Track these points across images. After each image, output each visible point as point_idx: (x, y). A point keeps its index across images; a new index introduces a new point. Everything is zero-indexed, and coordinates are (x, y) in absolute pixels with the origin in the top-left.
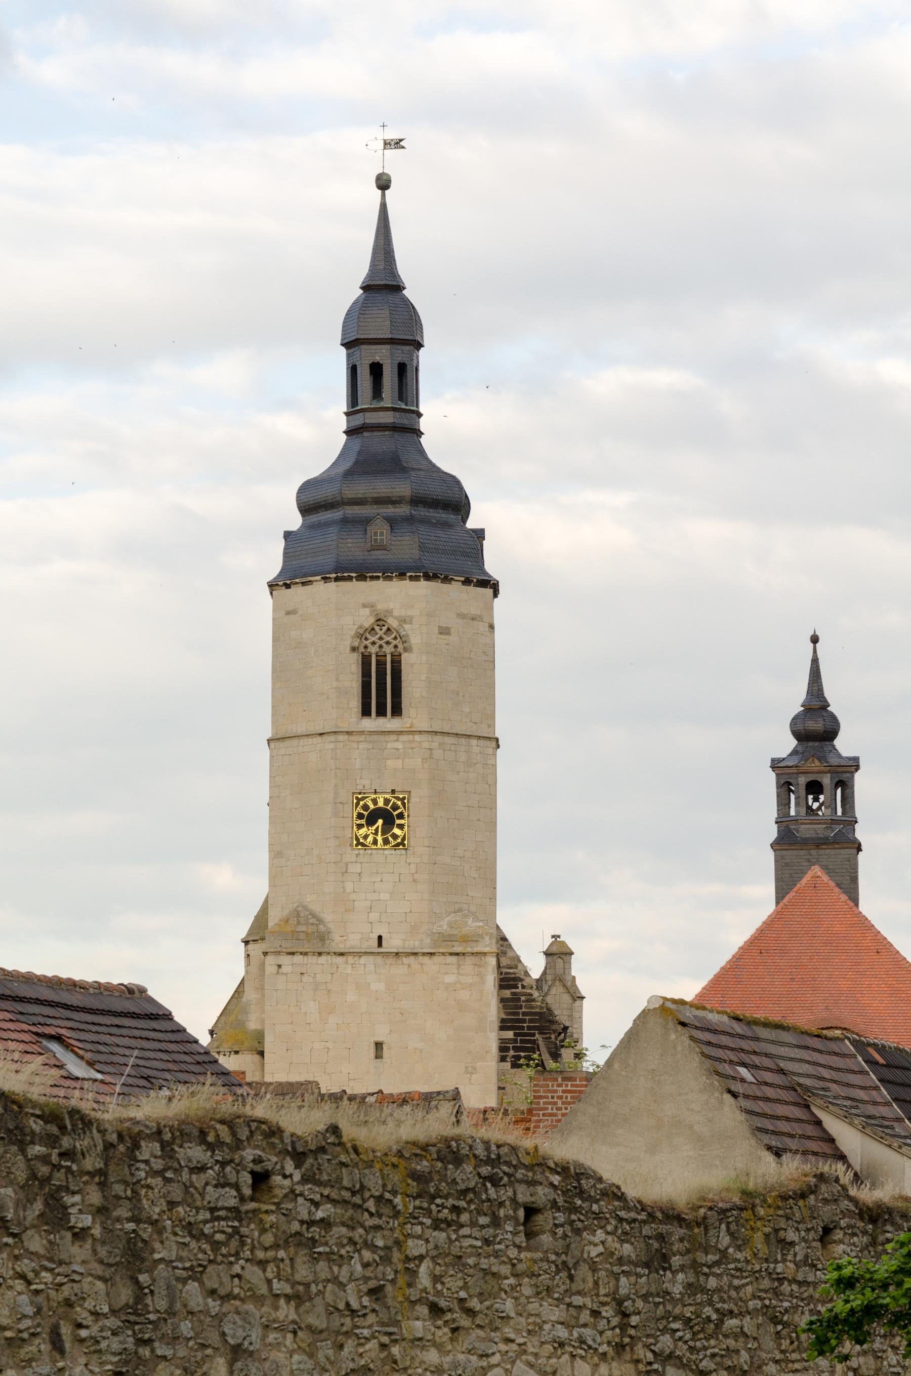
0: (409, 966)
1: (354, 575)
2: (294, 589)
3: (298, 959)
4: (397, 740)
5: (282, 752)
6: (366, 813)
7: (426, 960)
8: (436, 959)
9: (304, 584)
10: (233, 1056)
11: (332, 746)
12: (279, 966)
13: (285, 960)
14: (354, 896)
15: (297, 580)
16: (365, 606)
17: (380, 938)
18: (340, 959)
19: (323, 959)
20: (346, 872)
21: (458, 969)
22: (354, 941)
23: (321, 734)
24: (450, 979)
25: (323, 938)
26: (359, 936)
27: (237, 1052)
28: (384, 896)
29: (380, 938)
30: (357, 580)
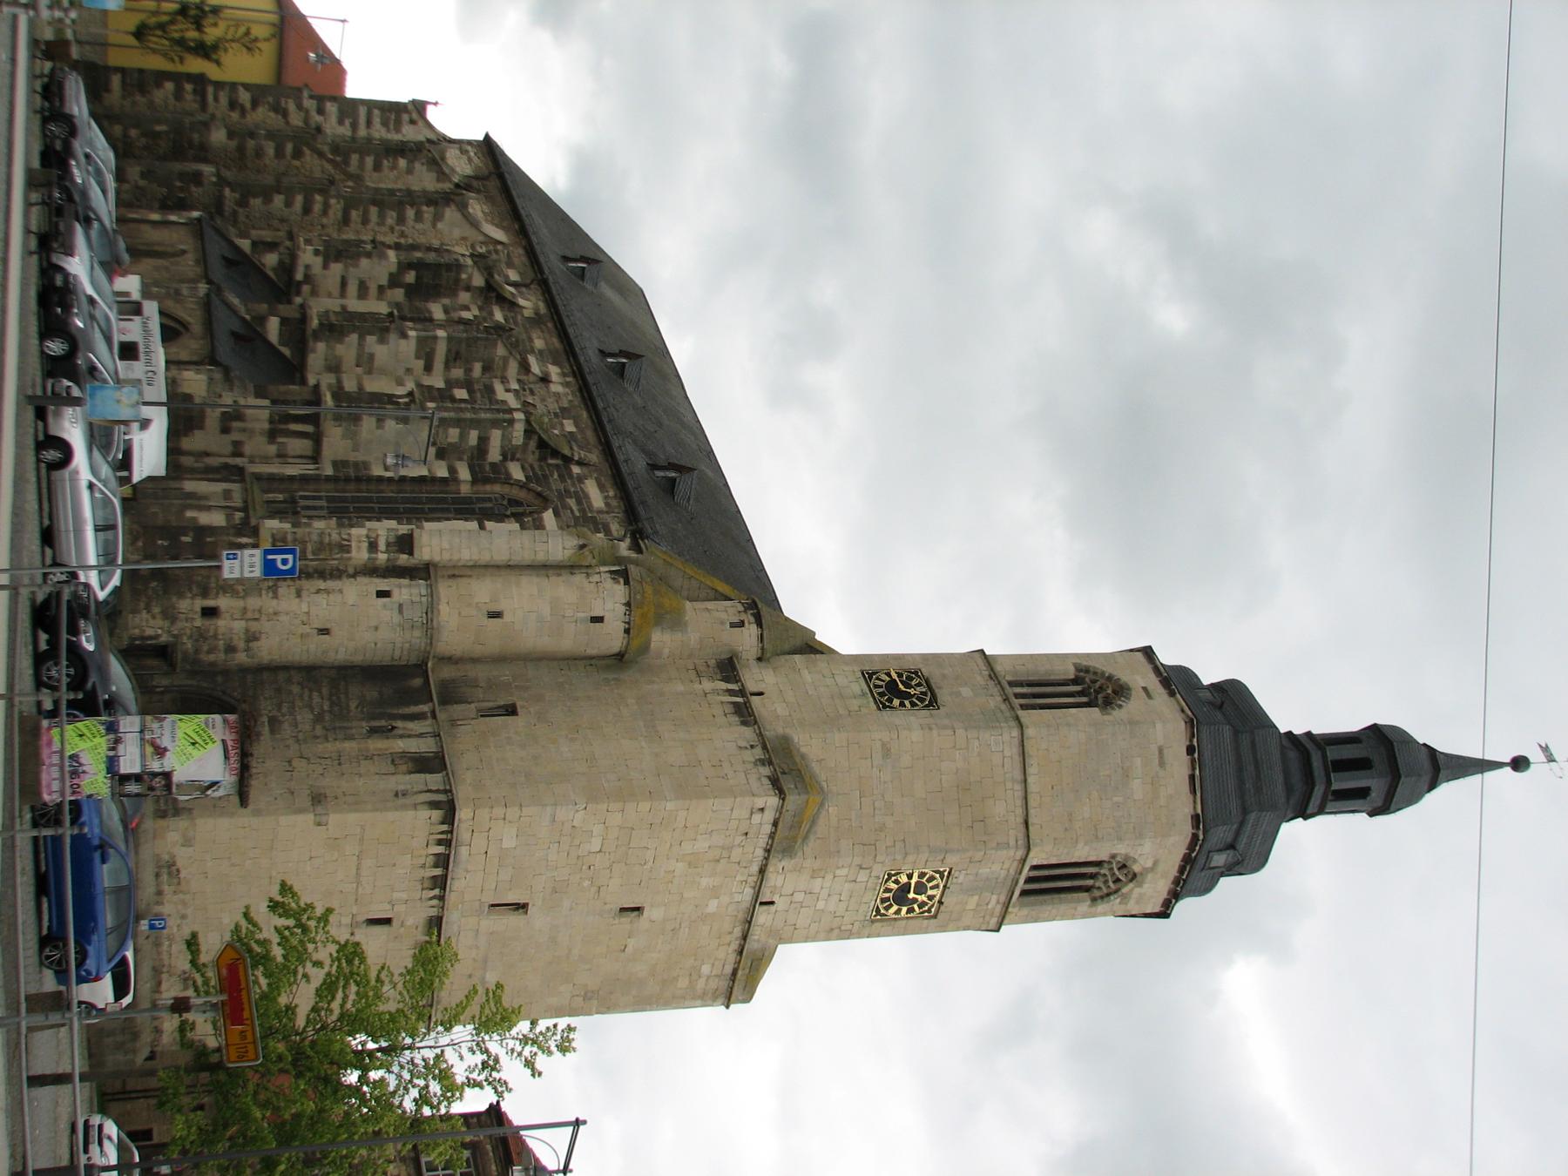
0: (730, 933)
1: (1193, 855)
2: (1185, 758)
3: (768, 829)
4: (998, 902)
5: (1007, 753)
6: (924, 880)
7: (735, 946)
8: (732, 958)
9: (1192, 777)
10: (622, 626)
11: (1012, 843)
12: (762, 810)
13: (769, 816)
14: (829, 877)
15: (1197, 772)
16: (1156, 863)
17: (772, 903)
18: (755, 868)
19: (760, 853)
20: (861, 868)
21: (716, 976)
22: (774, 878)
23: (1026, 823)
24: (706, 969)
25: (789, 851)
26: (779, 883)
27: (627, 631)
28: (821, 905)
29: (772, 903)
30: (1185, 854)
